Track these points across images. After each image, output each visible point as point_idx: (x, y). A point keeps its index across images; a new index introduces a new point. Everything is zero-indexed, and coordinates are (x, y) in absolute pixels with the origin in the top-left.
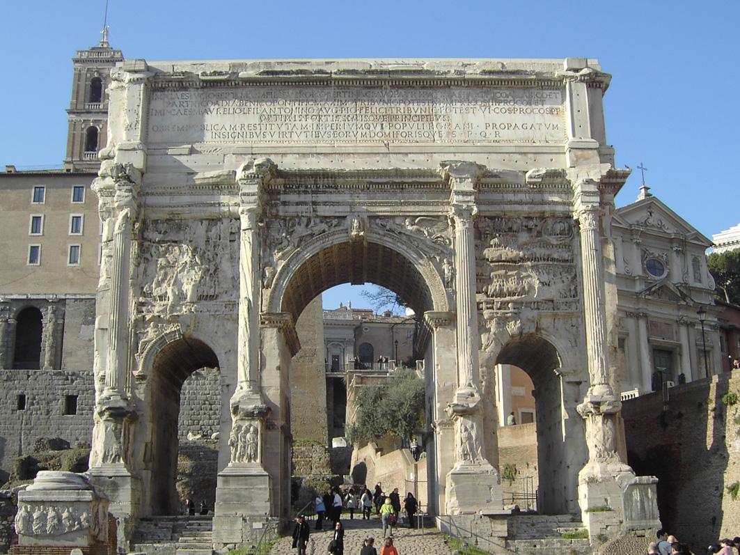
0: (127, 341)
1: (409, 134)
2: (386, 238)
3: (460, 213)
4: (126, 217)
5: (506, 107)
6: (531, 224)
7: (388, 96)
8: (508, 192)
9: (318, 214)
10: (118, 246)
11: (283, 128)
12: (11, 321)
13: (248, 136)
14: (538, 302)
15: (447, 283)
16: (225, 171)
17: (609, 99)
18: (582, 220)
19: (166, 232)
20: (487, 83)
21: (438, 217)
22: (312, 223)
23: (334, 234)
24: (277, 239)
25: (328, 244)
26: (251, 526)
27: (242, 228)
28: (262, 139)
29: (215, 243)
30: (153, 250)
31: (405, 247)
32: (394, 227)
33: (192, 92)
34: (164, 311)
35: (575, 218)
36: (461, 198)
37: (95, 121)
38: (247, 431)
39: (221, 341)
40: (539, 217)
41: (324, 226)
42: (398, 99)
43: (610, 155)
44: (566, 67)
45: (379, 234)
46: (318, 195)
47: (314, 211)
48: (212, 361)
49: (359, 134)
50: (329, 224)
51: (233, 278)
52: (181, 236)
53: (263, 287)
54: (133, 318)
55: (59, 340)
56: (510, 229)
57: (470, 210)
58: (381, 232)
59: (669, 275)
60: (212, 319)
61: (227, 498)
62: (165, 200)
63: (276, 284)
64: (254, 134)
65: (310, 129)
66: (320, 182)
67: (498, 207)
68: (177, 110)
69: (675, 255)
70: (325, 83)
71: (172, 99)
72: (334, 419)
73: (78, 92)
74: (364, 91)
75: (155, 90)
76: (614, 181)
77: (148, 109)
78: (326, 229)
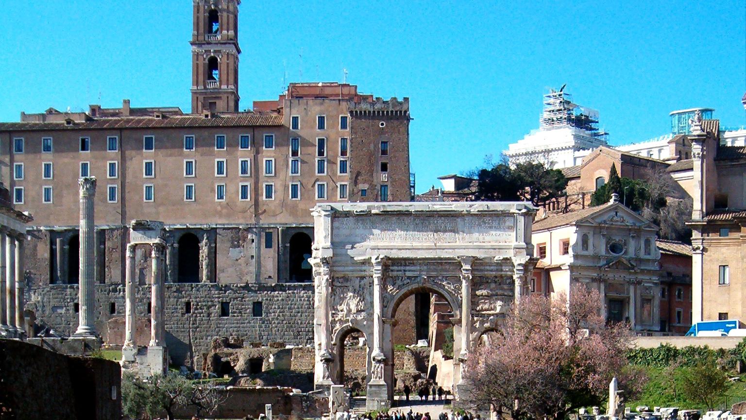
0: (330, 331)
3: (464, 278)
6: (496, 280)
11: (391, 236)
12: (176, 245)
16: (367, 257)
30: (337, 290)
33: (351, 218)
36: (465, 272)
37: (215, 52)
38: (378, 367)
41: (409, 281)
52: (348, 284)
54: (330, 319)
55: (213, 259)
56: (487, 282)
57: (468, 277)
59: (626, 253)
69: (631, 240)
75: (335, 217)
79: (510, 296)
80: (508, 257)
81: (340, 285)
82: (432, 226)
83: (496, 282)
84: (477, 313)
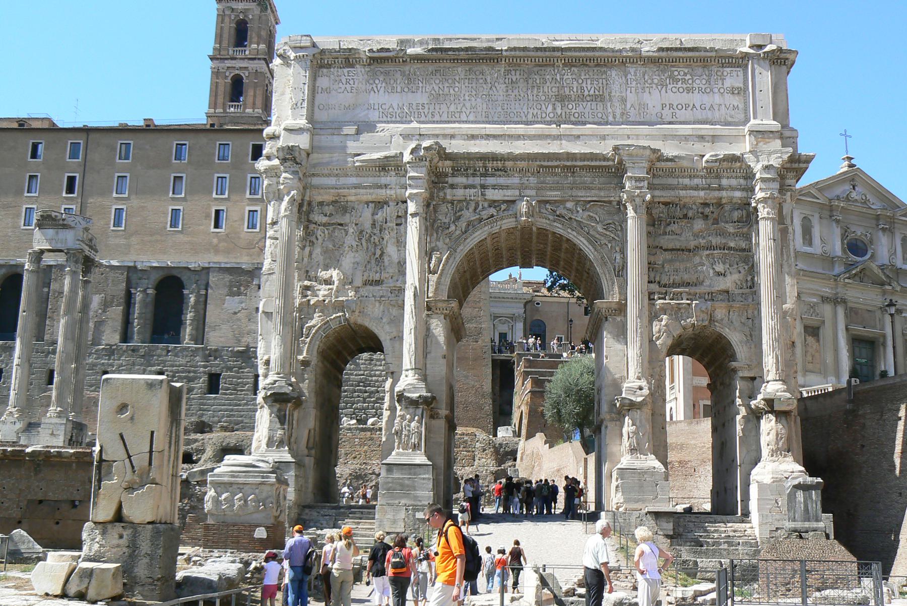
1: (581, 114)
2: (555, 224)
3: (632, 199)
4: (292, 201)
5: (685, 86)
6: (707, 211)
7: (560, 75)
8: (683, 177)
9: (486, 197)
10: (284, 230)
11: (452, 108)
13: (416, 116)
14: (712, 293)
15: (619, 272)
16: (392, 152)
17: (795, 79)
18: (760, 206)
19: (331, 215)
20: (664, 60)
21: (610, 202)
22: (481, 207)
23: (502, 219)
24: (444, 223)
25: (496, 229)
26: (414, 516)
27: (409, 212)
28: (431, 119)
29: (381, 226)
30: (319, 232)
31: (574, 233)
32: (564, 212)
33: (359, 69)
34: (330, 295)
35: (754, 205)
39: (387, 327)
40: (716, 203)
41: (493, 211)
42: (570, 77)
43: (793, 138)
44: (748, 44)
45: (549, 219)
46: (487, 178)
47: (482, 195)
48: (374, 345)
49: (530, 116)
50: (498, 209)
51: (399, 262)
52: (346, 219)
53: (430, 272)
54: (297, 302)
55: (202, 312)
58: (551, 217)
60: (377, 304)
61: (391, 487)
62: (331, 181)
63: (443, 270)
64: (422, 114)
65: (480, 109)
66: (490, 165)
67: (672, 193)
68: (343, 88)
69: (880, 233)
70: (496, 61)
71: (338, 76)
72: (500, 405)
73: (221, 36)
74: (536, 69)
75: (321, 67)
76: (796, 165)
77: (314, 86)
78: (495, 214)
79: (744, 250)
80: (738, 153)
81: (325, 220)
82: (550, 89)
83: (706, 217)
84: (663, 290)
